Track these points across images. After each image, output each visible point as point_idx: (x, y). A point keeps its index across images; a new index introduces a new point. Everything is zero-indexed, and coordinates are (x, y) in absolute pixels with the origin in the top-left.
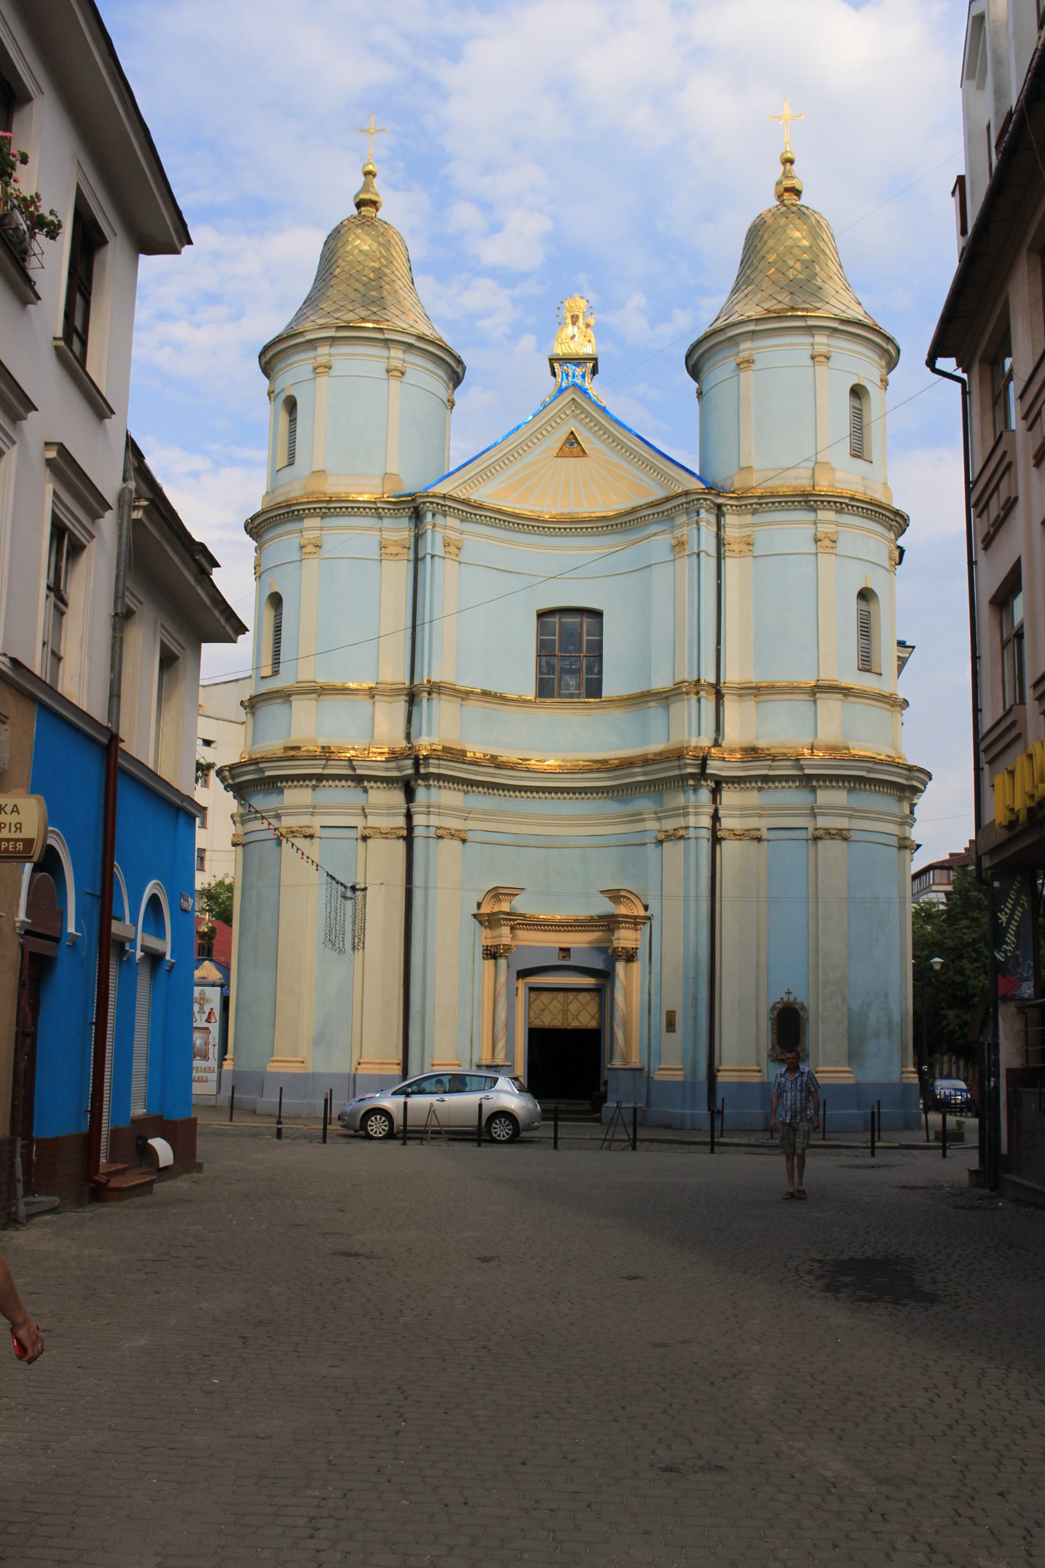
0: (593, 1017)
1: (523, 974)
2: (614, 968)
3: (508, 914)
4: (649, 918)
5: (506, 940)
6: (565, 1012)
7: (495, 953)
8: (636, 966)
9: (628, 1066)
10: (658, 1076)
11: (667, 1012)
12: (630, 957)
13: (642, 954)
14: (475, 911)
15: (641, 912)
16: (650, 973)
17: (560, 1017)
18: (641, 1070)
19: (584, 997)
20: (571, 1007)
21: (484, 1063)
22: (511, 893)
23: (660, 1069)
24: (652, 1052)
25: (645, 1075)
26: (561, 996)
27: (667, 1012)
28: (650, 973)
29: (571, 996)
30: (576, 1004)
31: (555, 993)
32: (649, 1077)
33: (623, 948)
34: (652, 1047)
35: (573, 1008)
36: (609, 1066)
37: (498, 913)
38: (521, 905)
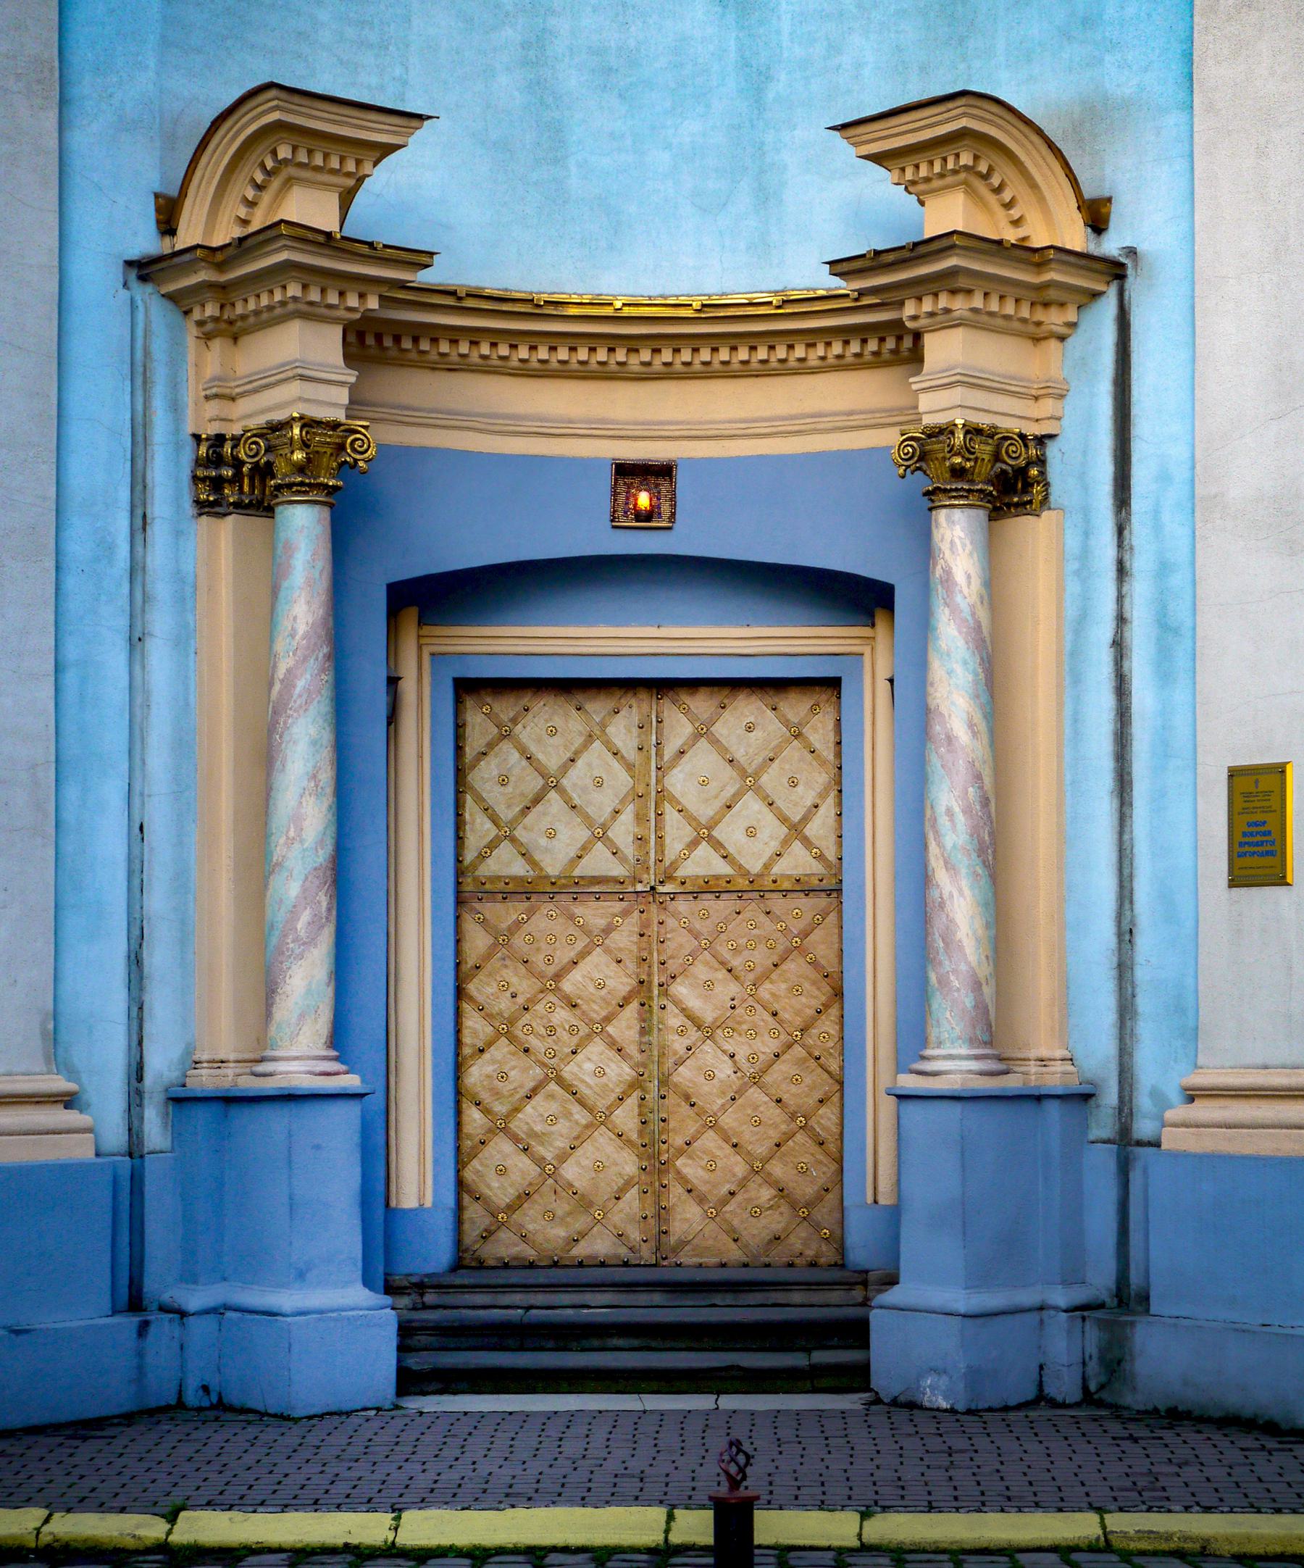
0: (796, 830)
1: (434, 598)
2: (924, 549)
3: (327, 241)
4: (1116, 271)
5: (330, 403)
6: (651, 800)
7: (265, 471)
8: (1033, 534)
9: (1011, 1083)
10: (1182, 1131)
11: (1234, 773)
12: (1007, 481)
13: (1080, 467)
14: (146, 242)
15: (1075, 236)
16: (1122, 571)
17: (623, 831)
18: (1084, 1098)
19: (748, 726)
20: (677, 781)
21: (205, 1081)
22: (349, 135)
23: (1191, 1095)
24: (1145, 1003)
25: (1103, 1124)
26: (623, 724)
27: (1234, 773)
28: (1122, 571)
29: (678, 722)
30: (703, 759)
31: (597, 707)
32: (1126, 1143)
33: (973, 431)
34: (1142, 974)
35: (695, 779)
36: (909, 1082)
37: (273, 232)
38: (410, 195)
